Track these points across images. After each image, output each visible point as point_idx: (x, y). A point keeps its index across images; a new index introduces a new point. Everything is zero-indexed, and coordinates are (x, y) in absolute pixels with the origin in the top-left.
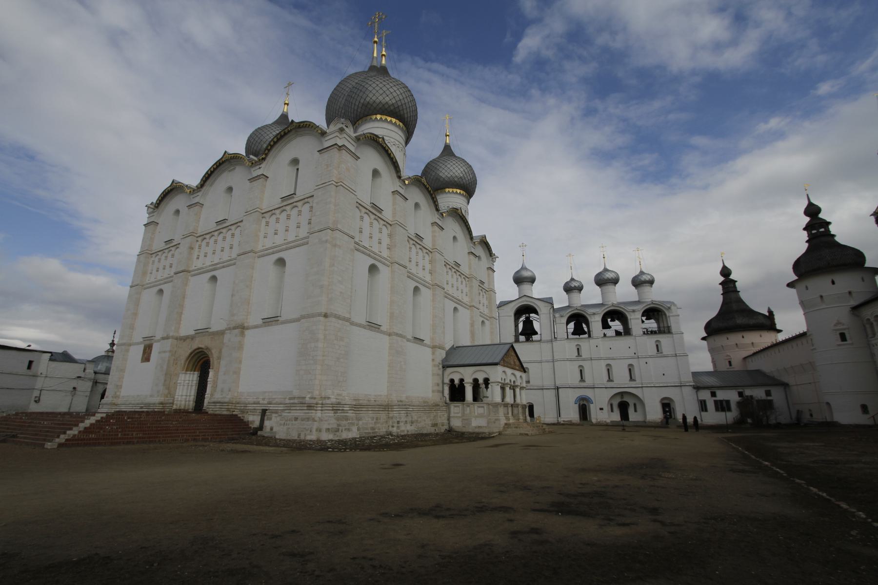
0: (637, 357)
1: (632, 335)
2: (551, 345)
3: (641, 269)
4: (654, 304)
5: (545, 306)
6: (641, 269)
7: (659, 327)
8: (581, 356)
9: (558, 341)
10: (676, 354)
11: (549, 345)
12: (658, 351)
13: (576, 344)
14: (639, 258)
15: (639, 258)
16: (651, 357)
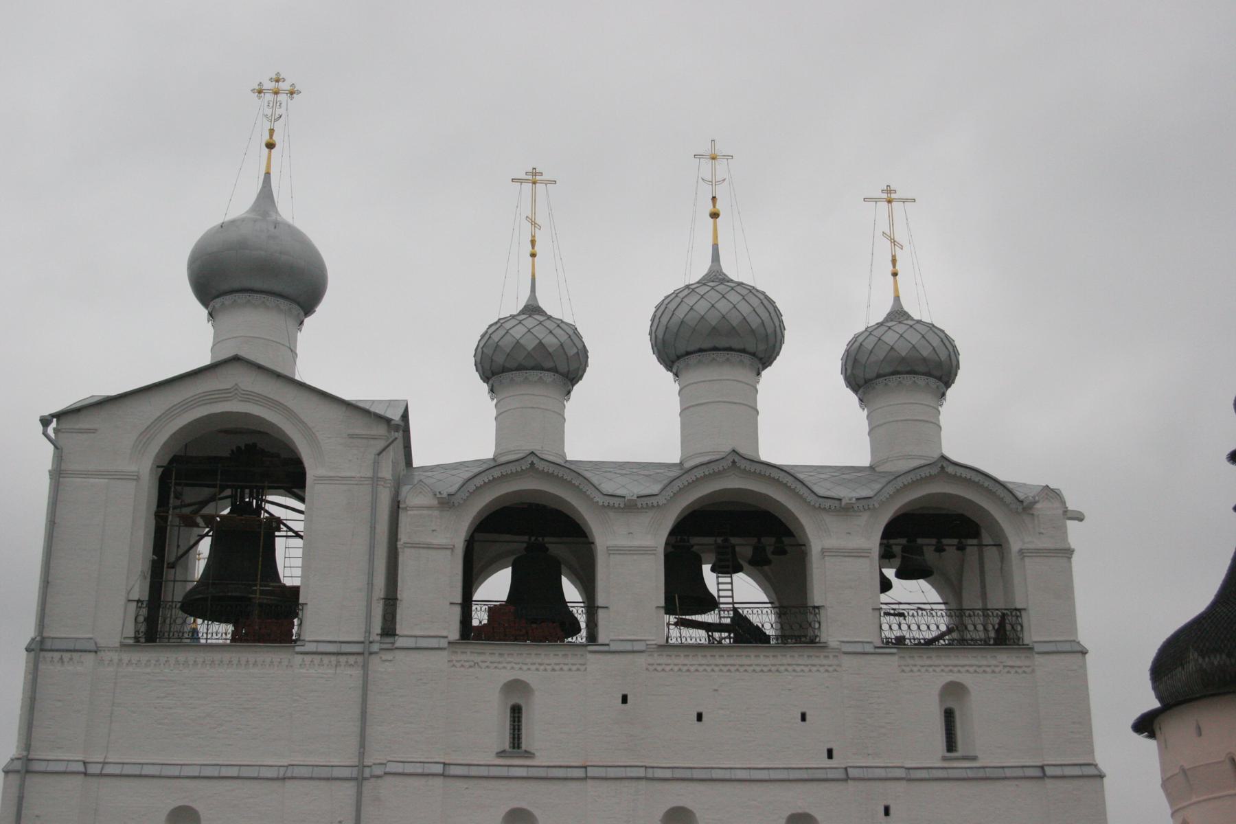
0: (841, 774)
1: (824, 647)
2: (357, 672)
3: (897, 298)
4: (956, 479)
5: (351, 436)
6: (897, 298)
7: (958, 613)
8: (529, 755)
9: (400, 655)
10: (1042, 767)
11: (350, 675)
12: (951, 745)
13: (508, 675)
14: (893, 242)
15: (894, 242)
16: (910, 777)
